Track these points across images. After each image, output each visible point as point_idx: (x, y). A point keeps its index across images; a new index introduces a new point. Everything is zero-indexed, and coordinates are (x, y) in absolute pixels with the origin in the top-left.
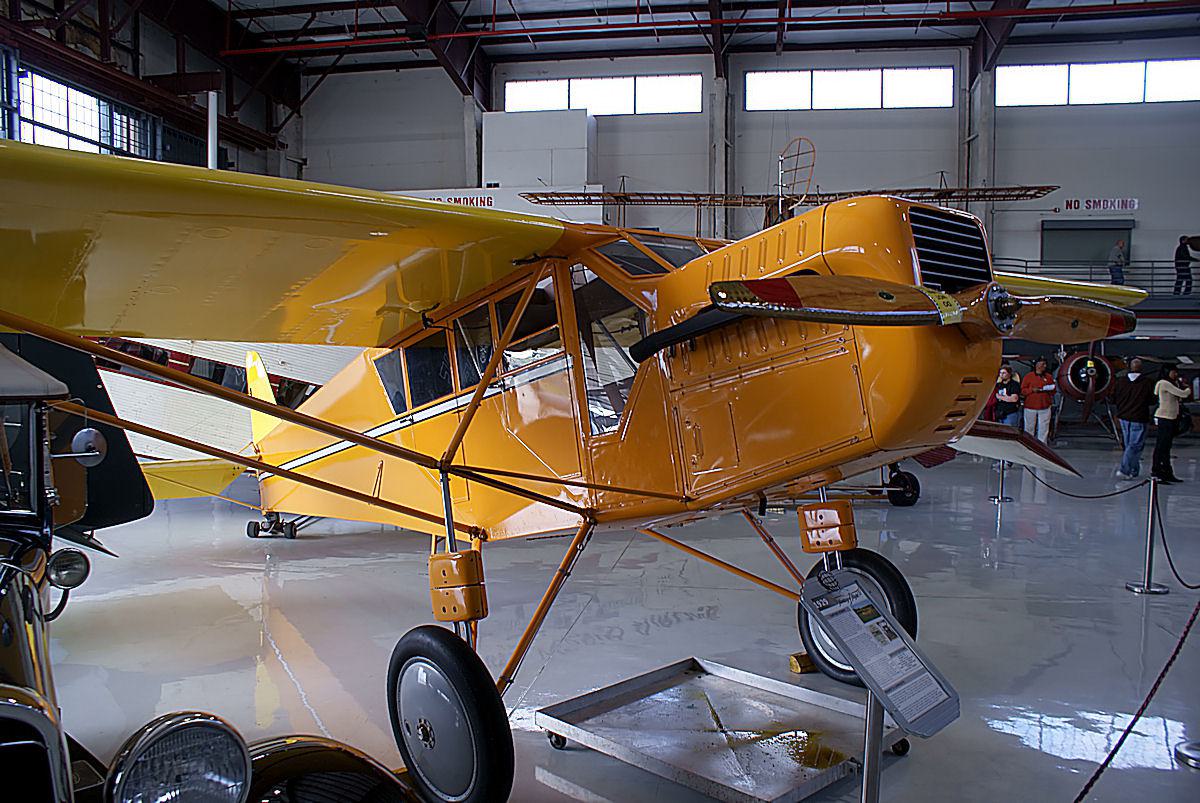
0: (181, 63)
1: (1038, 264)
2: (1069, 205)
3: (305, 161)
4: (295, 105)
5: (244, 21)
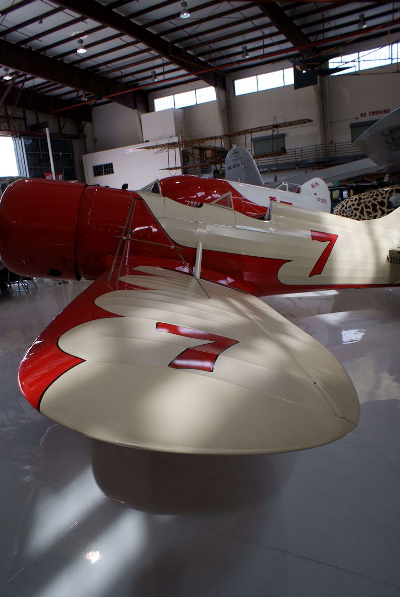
0: (38, 119)
1: (351, 143)
2: (362, 115)
3: (96, 139)
4: (91, 120)
5: (60, 98)
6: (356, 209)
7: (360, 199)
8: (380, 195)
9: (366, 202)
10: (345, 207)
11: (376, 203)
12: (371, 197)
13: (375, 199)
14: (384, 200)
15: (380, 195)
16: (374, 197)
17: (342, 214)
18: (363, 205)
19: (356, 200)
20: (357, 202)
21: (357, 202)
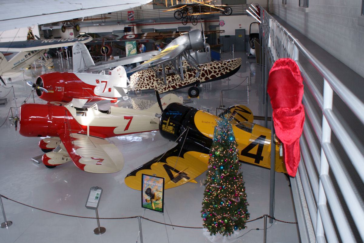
6: (141, 78)
7: (143, 73)
8: (152, 72)
9: (145, 75)
10: (136, 77)
11: (150, 76)
12: (148, 73)
13: (150, 74)
14: (154, 74)
15: (152, 72)
16: (149, 72)
17: (135, 80)
18: (144, 76)
19: (141, 73)
20: (141, 74)
21: (141, 74)
